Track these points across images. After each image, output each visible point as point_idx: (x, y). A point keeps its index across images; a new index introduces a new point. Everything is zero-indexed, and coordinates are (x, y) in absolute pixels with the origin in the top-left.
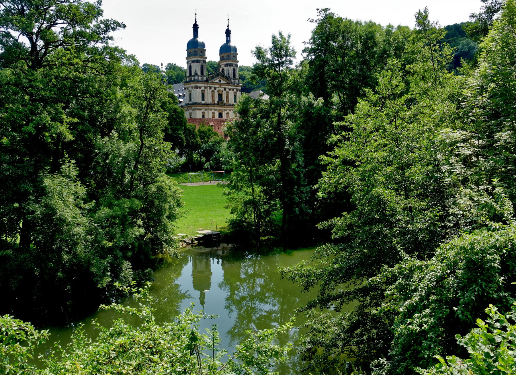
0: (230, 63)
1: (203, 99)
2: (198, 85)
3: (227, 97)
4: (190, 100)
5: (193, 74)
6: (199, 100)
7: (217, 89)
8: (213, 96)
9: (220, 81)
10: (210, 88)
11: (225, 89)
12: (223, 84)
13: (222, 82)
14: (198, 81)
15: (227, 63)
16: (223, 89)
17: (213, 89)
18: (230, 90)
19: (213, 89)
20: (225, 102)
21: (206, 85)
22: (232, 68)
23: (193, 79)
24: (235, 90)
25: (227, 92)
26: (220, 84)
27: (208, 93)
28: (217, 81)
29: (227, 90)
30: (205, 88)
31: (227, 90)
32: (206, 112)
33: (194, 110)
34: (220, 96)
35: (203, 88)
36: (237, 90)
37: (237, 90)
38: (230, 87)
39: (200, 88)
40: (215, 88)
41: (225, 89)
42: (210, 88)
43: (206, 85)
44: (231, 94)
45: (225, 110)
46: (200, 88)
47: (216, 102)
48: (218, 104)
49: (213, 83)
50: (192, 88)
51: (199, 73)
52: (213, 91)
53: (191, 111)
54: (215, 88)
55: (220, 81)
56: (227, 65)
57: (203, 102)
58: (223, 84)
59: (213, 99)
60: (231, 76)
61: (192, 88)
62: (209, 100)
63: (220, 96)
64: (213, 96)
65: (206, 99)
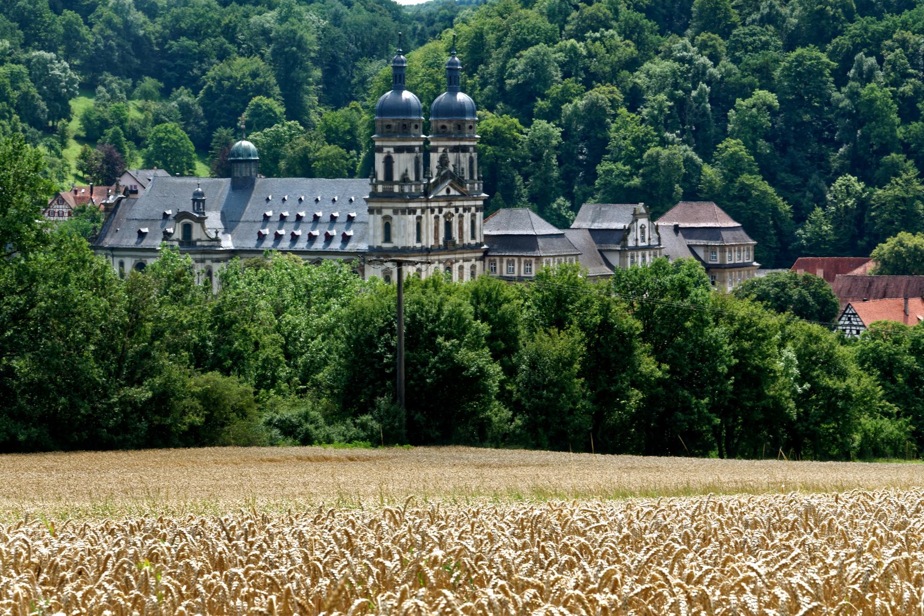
0: (463, 143)
1: (419, 239)
2: (411, 205)
4: (387, 238)
5: (396, 177)
6: (412, 242)
7: (445, 210)
9: (448, 191)
10: (433, 211)
11: (457, 211)
12: (455, 198)
14: (413, 198)
15: (457, 143)
16: (453, 210)
18: (464, 211)
21: (424, 205)
22: (468, 155)
23: (396, 189)
24: (473, 209)
25: (461, 216)
26: (449, 199)
28: (443, 193)
29: (461, 210)
30: (423, 211)
31: (461, 210)
34: (448, 225)
35: (419, 212)
36: (477, 210)
37: (477, 210)
38: (466, 203)
39: (414, 212)
40: (440, 212)
41: (457, 211)
42: (433, 211)
43: (424, 205)
45: (457, 261)
46: (414, 212)
47: (441, 243)
49: (437, 199)
50: (396, 211)
51: (412, 177)
52: (437, 218)
54: (440, 212)
55: (448, 191)
57: (419, 245)
58: (455, 198)
62: (429, 241)
63: (448, 225)
65: (424, 237)
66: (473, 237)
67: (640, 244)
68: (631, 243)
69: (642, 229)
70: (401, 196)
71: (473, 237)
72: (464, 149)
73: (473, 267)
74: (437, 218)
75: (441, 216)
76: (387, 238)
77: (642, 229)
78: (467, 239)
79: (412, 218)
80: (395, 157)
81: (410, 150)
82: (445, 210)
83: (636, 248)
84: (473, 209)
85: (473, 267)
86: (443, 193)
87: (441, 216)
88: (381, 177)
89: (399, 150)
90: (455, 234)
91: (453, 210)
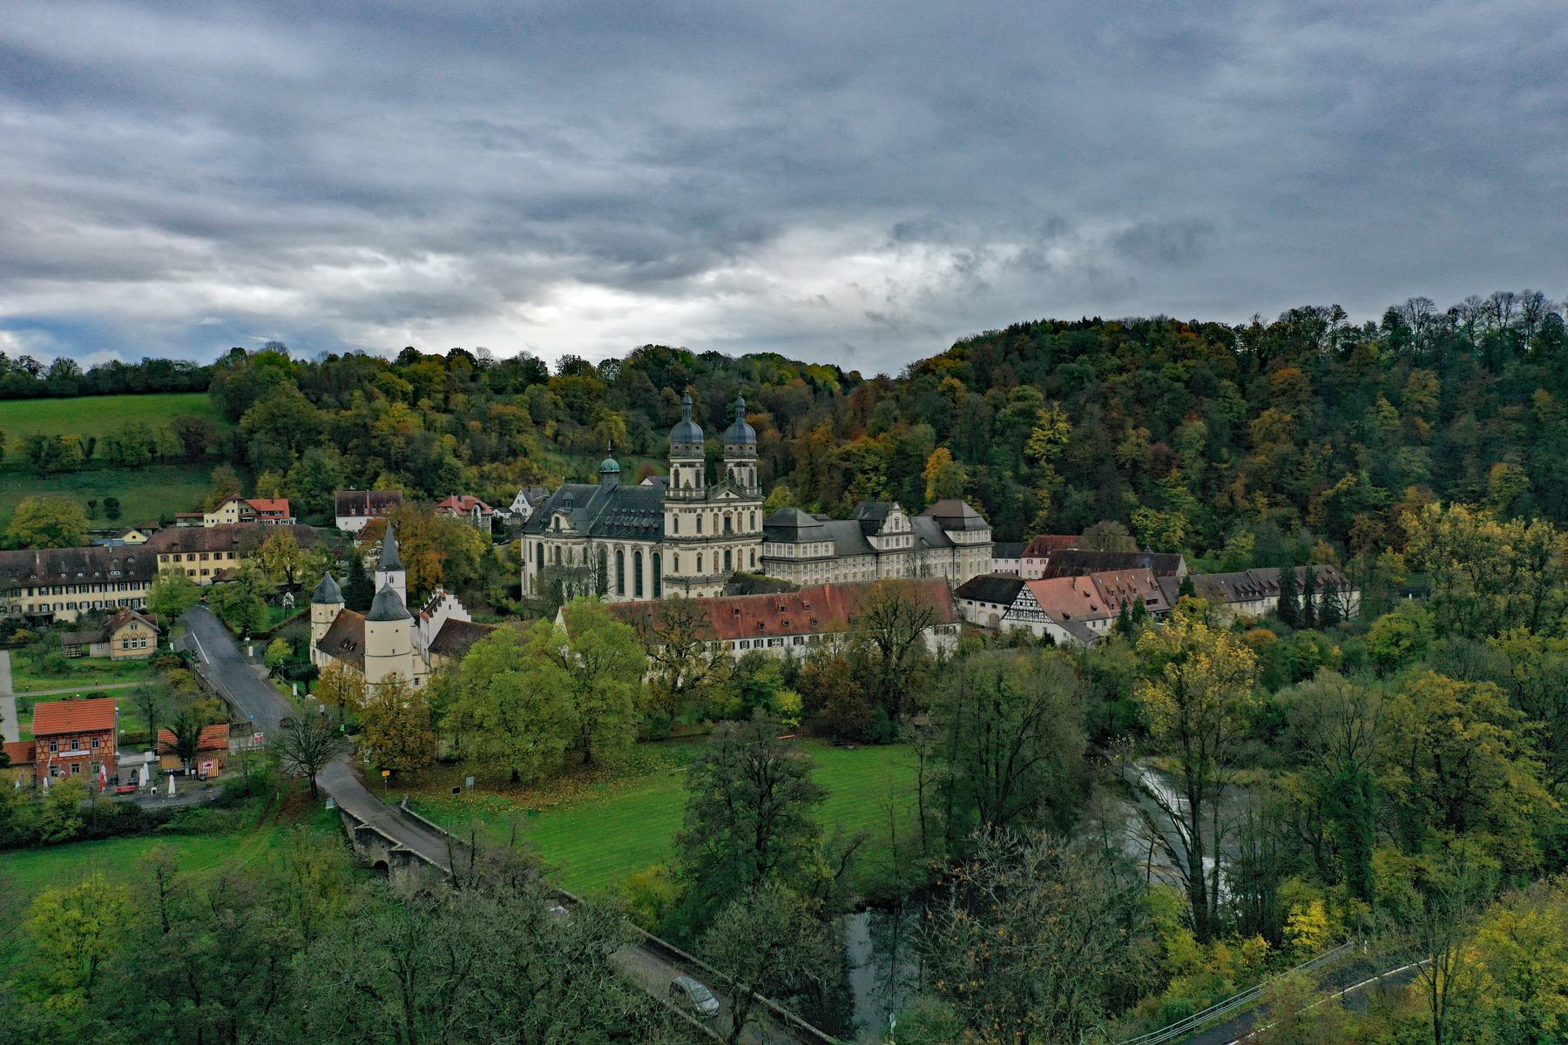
1: (699, 530)
3: (740, 523)
5: (681, 486)
6: (693, 533)
7: (724, 510)
8: (716, 523)
10: (712, 510)
12: (733, 500)
13: (732, 496)
14: (692, 501)
16: (732, 509)
17: (716, 510)
19: (716, 510)
20: (736, 532)
24: (752, 508)
25: (740, 514)
26: (728, 501)
27: (708, 518)
29: (740, 509)
30: (703, 510)
31: (740, 509)
32: (704, 552)
33: (682, 549)
34: (728, 521)
35: (699, 511)
42: (712, 510)
44: (746, 515)
47: (721, 533)
48: (724, 538)
49: (717, 501)
50: (681, 511)
51: (693, 485)
52: (716, 515)
53: (676, 550)
56: (738, 465)
57: (699, 535)
58: (733, 500)
59: (716, 530)
60: (746, 483)
61: (681, 511)
62: (708, 531)
63: (728, 521)
64: (716, 523)
66: (752, 527)
67: (894, 531)
68: (886, 529)
69: (897, 521)
70: (684, 500)
71: (752, 527)
72: (745, 465)
73: (753, 550)
74: (716, 515)
75: (721, 514)
76: (676, 530)
77: (897, 521)
78: (746, 529)
79: (693, 516)
80: (680, 469)
81: (691, 465)
82: (724, 510)
83: (891, 534)
84: (752, 508)
85: (753, 550)
86: (723, 496)
87: (721, 514)
88: (672, 485)
89: (683, 465)
90: (734, 526)
91: (732, 509)
